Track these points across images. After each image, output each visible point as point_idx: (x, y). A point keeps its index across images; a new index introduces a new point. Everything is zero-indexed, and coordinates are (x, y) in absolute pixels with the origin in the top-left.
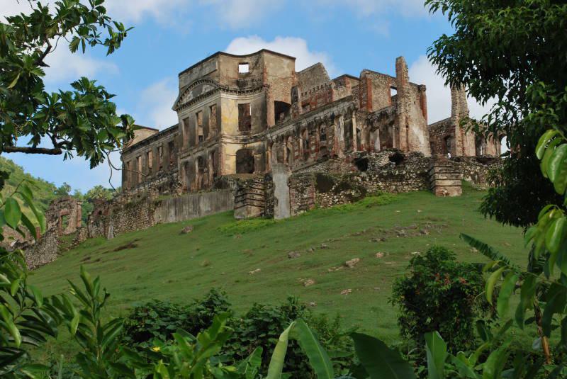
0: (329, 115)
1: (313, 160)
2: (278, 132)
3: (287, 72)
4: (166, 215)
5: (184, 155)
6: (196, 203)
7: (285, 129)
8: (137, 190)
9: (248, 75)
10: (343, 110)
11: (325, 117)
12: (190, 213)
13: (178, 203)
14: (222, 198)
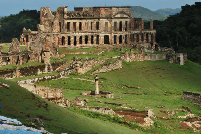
0: (150, 32)
2: (135, 32)
4: (148, 58)
6: (155, 56)
11: (149, 32)
14: (161, 56)
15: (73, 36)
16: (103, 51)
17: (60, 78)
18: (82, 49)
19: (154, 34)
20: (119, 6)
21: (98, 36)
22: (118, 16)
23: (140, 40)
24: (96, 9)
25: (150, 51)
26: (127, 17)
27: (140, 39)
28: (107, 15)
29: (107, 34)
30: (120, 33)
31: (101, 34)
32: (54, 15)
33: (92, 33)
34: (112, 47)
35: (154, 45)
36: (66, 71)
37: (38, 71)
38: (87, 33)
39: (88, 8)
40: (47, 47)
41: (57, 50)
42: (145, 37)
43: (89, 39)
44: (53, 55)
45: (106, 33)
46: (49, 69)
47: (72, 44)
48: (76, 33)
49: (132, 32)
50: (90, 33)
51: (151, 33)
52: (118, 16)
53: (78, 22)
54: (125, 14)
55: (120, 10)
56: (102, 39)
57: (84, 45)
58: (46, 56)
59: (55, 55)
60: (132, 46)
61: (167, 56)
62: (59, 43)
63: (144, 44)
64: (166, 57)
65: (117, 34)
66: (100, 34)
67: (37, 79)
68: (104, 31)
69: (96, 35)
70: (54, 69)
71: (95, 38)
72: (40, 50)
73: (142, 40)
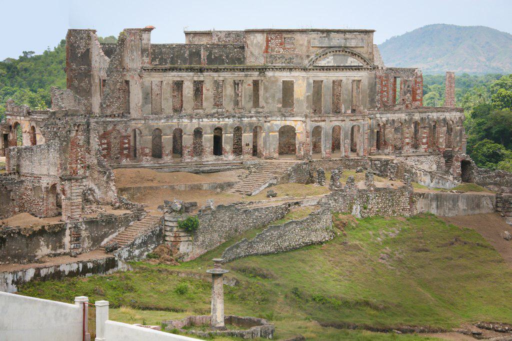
0: (442, 117)
2: (389, 115)
5: (316, 119)
7: (396, 115)
8: (175, 121)
10: (455, 118)
12: (449, 209)
13: (439, 199)
15: (170, 127)
16: (271, 182)
17: (116, 269)
18: (203, 172)
19: (457, 122)
20: (330, 28)
21: (256, 131)
22: (328, 62)
23: (408, 144)
24: (252, 37)
25: (439, 183)
26: (361, 64)
27: (407, 140)
28: (291, 58)
29: (289, 122)
30: (334, 119)
31: (269, 122)
32: (109, 57)
33: (239, 118)
34: (304, 166)
35: (457, 160)
36: (137, 248)
37: (38, 246)
38: (219, 119)
39: (229, 34)
40: (74, 166)
41: (110, 173)
42: (424, 134)
43: (227, 137)
44: (97, 191)
45: (287, 118)
46: (77, 238)
47: (167, 155)
48: (181, 117)
49: (378, 116)
50: (231, 120)
51: (444, 120)
52: (329, 61)
53: (188, 79)
54: (353, 54)
55: (337, 40)
56: (271, 139)
57: (209, 158)
58: (69, 196)
59: (106, 192)
60: (375, 164)
61: (497, 202)
62: (121, 153)
63: (422, 159)
64: (494, 203)
65: (322, 124)
66: (265, 122)
67: (31, 273)
68: (280, 111)
69: (250, 125)
70: (96, 241)
71: (247, 137)
72: (49, 175)
73: (416, 146)
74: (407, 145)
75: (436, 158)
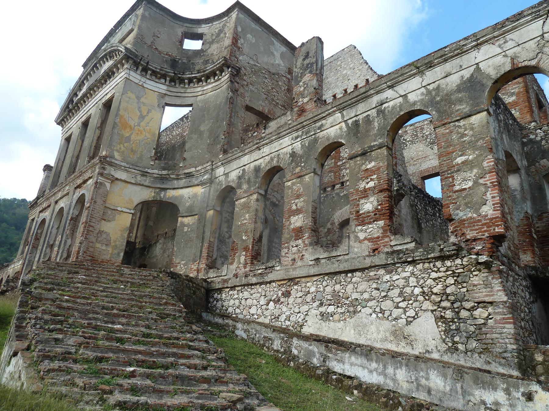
0: (454, 80)
1: (367, 246)
3: (279, 65)
7: (266, 150)
9: (196, 53)
23: (298, 233)
74: (297, 238)
75: (437, 277)
